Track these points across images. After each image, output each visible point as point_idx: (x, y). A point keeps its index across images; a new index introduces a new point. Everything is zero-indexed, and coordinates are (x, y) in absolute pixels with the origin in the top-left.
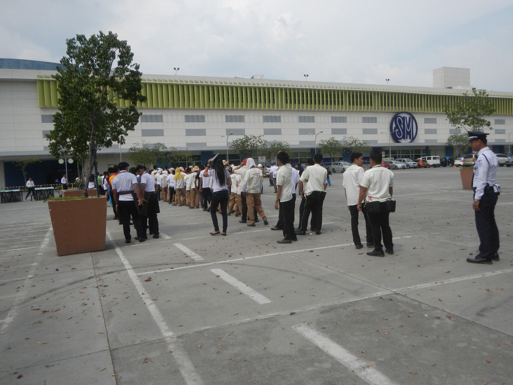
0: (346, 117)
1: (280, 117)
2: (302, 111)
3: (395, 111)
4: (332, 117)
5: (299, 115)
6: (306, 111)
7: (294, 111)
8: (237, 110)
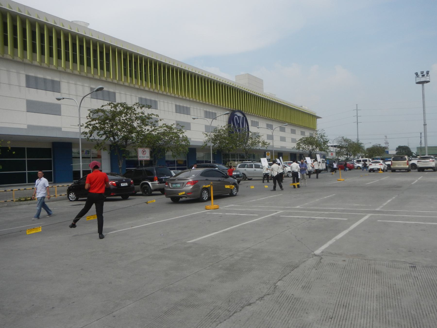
0: (189, 108)
1: (115, 93)
2: (144, 90)
3: (232, 109)
4: (176, 105)
5: (139, 96)
6: (149, 91)
7: (134, 88)
8: (48, 69)
